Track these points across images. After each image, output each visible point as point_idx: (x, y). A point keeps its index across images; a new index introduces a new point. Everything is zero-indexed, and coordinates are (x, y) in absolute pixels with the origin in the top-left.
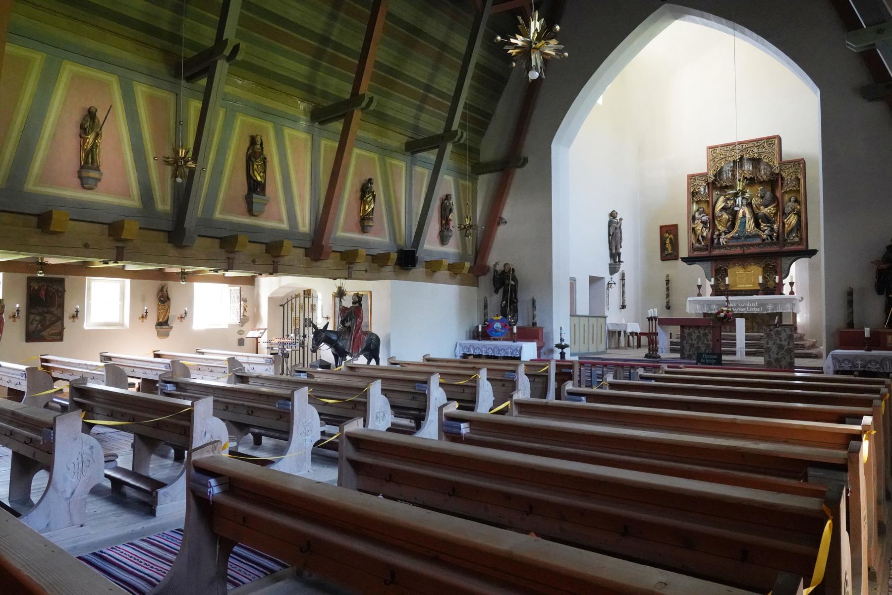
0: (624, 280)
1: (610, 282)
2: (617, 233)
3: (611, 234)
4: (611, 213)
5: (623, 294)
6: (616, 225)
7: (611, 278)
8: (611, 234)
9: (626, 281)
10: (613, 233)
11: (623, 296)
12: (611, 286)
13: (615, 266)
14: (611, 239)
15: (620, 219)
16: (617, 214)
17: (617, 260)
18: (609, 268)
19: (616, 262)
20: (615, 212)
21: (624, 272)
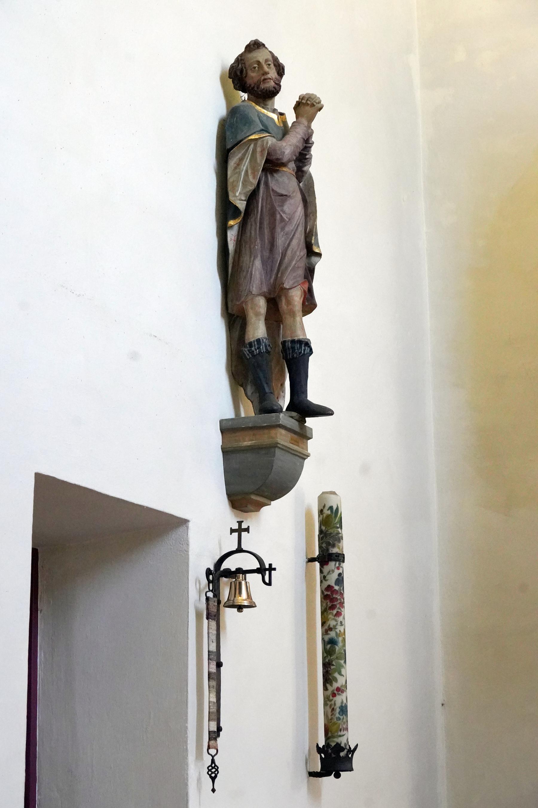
0: (340, 558)
1: (230, 564)
2: (284, 197)
3: (242, 205)
4: (240, 60)
5: (327, 665)
6: (271, 141)
7: (240, 530)
8: (242, 205)
9: (347, 567)
10: (252, 198)
11: (328, 679)
12: (237, 589)
13: (264, 439)
14: (239, 242)
15: (298, 106)
16: (280, 70)
17: (286, 401)
18: (226, 452)
19: (276, 410)
20: (260, 56)
21: (333, 502)
